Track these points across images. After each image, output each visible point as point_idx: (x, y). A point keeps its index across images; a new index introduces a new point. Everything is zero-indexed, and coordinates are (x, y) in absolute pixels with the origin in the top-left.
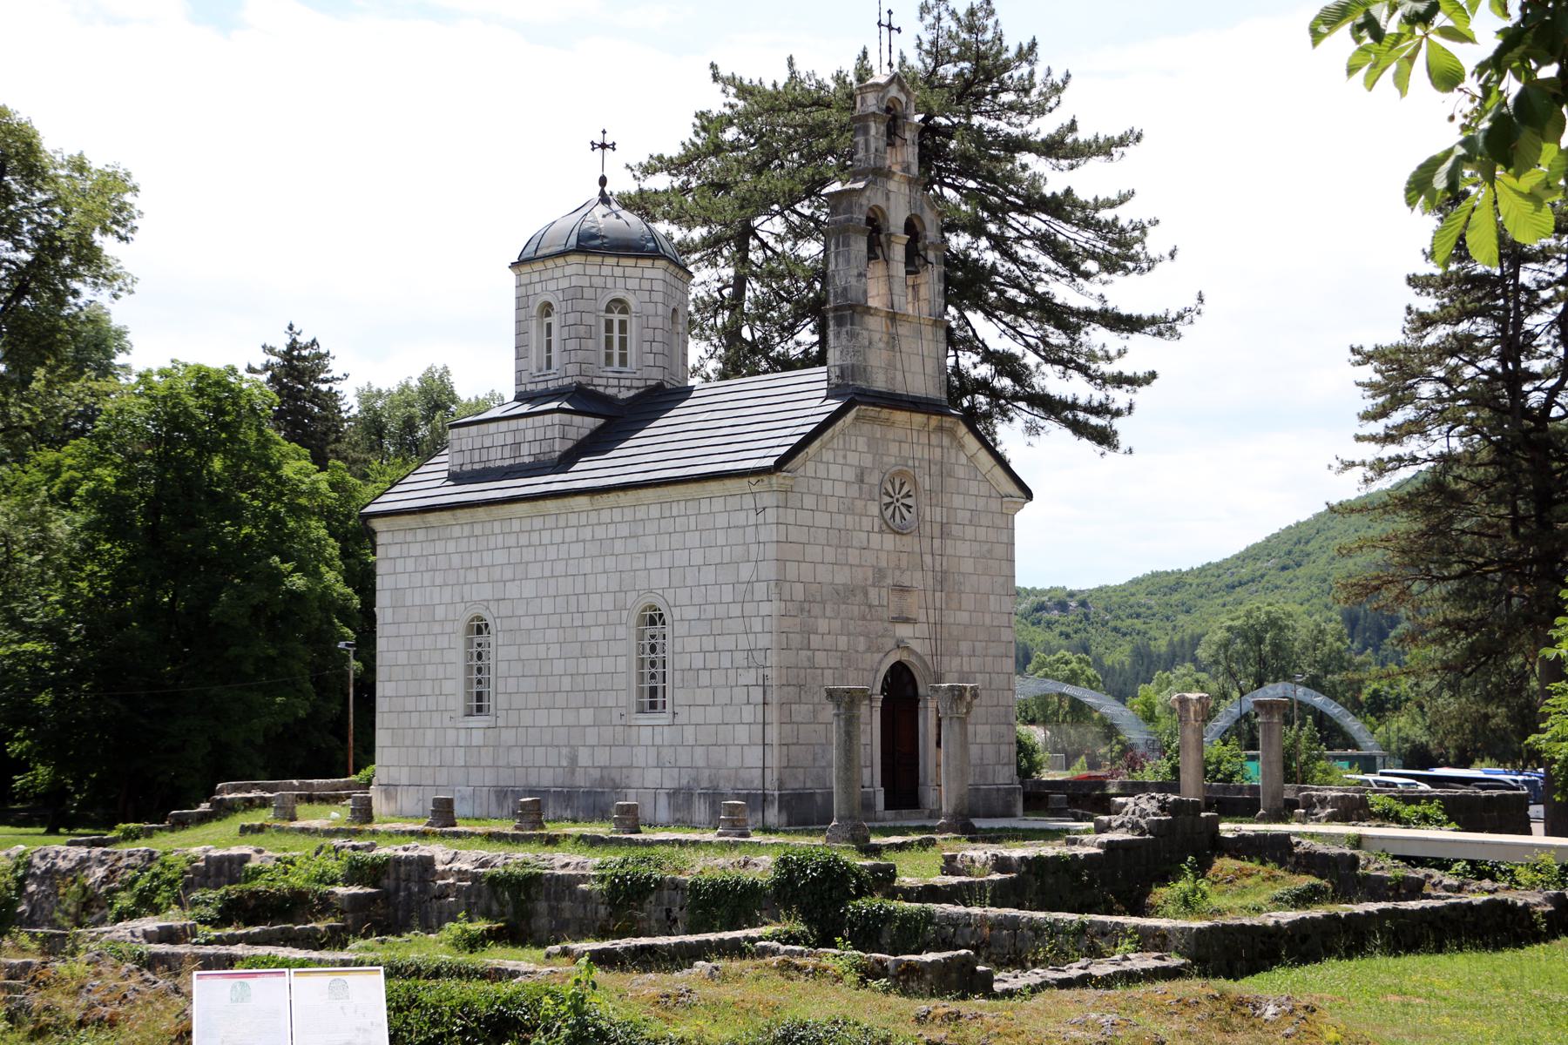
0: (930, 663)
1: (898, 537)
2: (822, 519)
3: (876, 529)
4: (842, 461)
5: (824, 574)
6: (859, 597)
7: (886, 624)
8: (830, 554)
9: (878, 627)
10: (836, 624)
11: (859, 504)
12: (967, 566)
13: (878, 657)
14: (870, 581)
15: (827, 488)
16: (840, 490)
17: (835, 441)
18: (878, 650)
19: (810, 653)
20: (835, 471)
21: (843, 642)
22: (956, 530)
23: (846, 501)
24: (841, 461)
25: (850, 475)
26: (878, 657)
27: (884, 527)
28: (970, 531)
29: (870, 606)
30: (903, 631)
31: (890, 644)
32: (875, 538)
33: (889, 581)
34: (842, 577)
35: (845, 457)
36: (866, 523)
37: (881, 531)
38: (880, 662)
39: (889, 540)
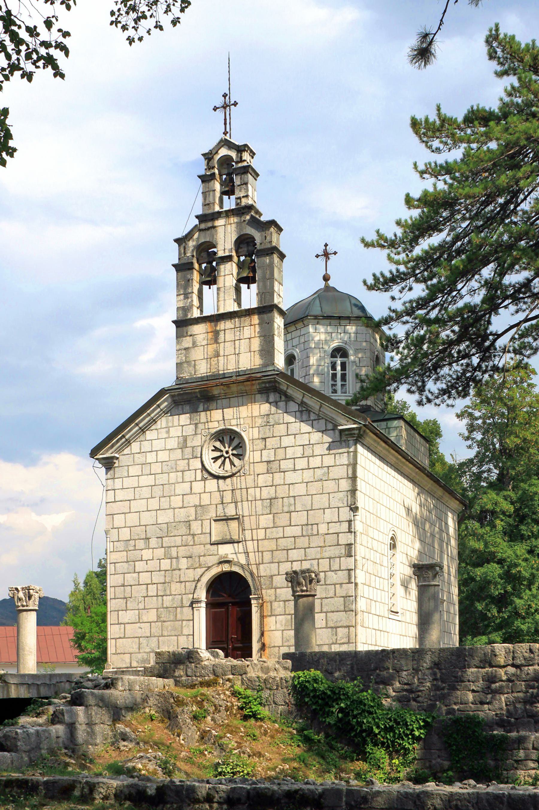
0: (255, 571)
1: (221, 481)
2: (148, 480)
3: (199, 477)
4: (165, 435)
5: (147, 518)
6: (183, 530)
7: (209, 546)
8: (154, 504)
9: (198, 550)
10: (160, 552)
11: (182, 464)
12: (300, 489)
13: (200, 571)
14: (193, 517)
15: (151, 458)
16: (163, 456)
17: (159, 422)
18: (200, 566)
19: (136, 575)
20: (158, 445)
21: (166, 564)
22: (286, 465)
23: (169, 463)
24: (165, 435)
25: (173, 443)
26: (200, 571)
27: (206, 475)
28: (301, 463)
29: (194, 535)
30: (226, 550)
31: (214, 560)
32: (198, 487)
33: (212, 514)
34: (164, 517)
35: (168, 432)
36: (189, 476)
37: (204, 479)
38: (201, 576)
39: (212, 484)
